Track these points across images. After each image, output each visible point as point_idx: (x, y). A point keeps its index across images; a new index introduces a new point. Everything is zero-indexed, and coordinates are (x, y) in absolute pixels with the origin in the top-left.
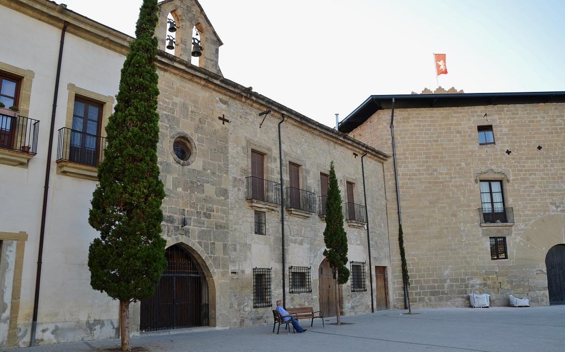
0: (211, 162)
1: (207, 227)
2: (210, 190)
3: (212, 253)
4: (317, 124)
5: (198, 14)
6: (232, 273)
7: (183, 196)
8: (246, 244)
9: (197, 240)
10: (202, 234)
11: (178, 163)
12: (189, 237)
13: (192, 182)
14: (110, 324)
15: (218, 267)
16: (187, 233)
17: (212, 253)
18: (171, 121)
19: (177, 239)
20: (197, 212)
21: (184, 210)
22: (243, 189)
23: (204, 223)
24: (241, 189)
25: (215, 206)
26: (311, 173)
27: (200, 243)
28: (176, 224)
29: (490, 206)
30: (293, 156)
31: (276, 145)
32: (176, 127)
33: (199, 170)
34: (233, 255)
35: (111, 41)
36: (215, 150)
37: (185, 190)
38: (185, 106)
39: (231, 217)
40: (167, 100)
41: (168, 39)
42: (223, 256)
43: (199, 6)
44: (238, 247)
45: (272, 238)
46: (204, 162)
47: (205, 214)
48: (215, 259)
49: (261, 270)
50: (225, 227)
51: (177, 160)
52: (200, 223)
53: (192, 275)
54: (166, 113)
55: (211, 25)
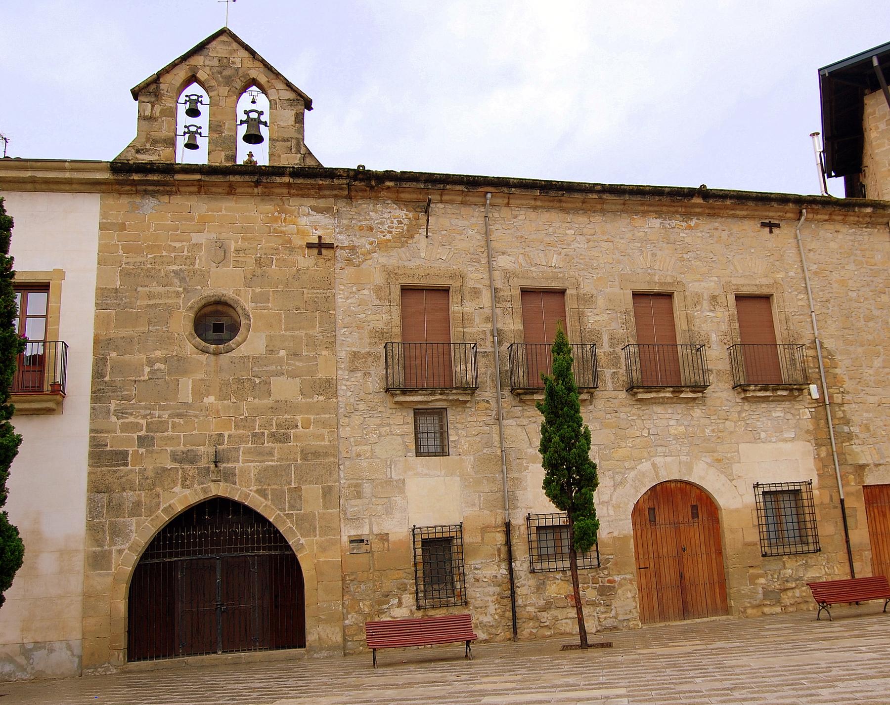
0: (288, 333)
1: (279, 460)
2: (285, 388)
3: (292, 507)
4: (599, 188)
5: (249, 63)
6: (351, 541)
7: (218, 411)
8: (389, 482)
9: (255, 488)
10: (265, 476)
11: (204, 351)
12: (235, 484)
13: (240, 381)
14: (65, 649)
15: (310, 531)
16: (229, 476)
17: (292, 507)
18: (188, 279)
19: (204, 490)
20: (254, 435)
22: (378, 371)
23: (271, 454)
24: (372, 372)
25: (298, 417)
26: (601, 302)
27: (262, 493)
28: (203, 464)
29: (423, 428)
30: (534, 275)
31: (479, 262)
32: (199, 287)
34: (353, 506)
35: (46, 181)
36: (298, 309)
37: (223, 397)
38: (222, 246)
39: (345, 432)
40: (178, 245)
41: (242, 122)
42: (321, 511)
43: (247, 48)
44: (367, 489)
45: (469, 460)
46: (270, 338)
47: (273, 435)
48: (301, 520)
50: (326, 454)
51: (200, 348)
52: (260, 454)
53: (261, 552)
54: (175, 267)
55: (278, 75)
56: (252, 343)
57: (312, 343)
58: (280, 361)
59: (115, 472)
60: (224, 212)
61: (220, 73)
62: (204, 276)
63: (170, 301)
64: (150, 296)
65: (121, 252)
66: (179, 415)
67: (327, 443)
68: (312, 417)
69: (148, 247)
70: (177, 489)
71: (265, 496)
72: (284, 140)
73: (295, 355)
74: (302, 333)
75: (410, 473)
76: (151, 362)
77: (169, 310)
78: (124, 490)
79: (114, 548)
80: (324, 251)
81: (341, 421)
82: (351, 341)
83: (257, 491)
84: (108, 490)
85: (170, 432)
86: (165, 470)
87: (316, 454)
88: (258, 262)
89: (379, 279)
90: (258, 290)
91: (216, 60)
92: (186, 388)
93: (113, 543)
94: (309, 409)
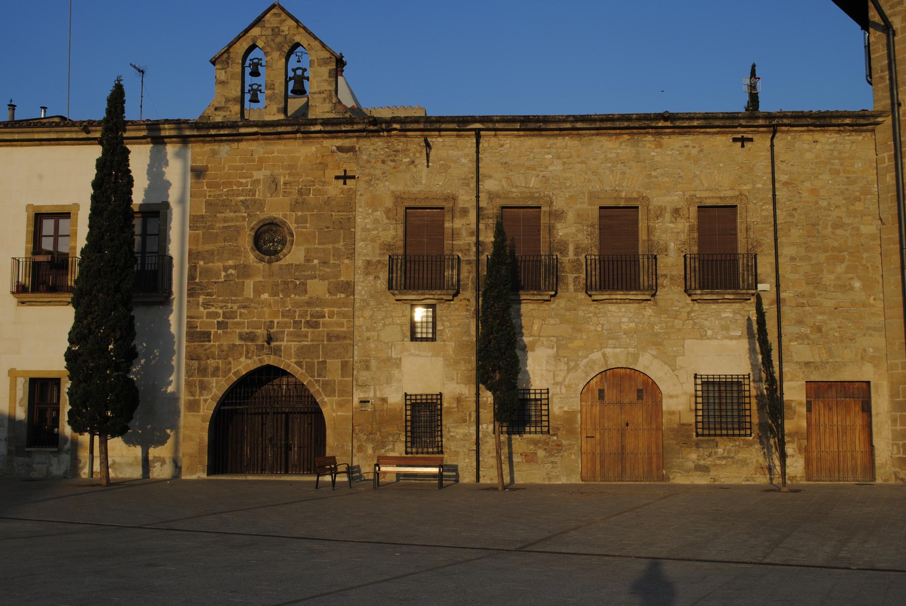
1: (312, 340)
2: (317, 288)
3: (319, 375)
4: (571, 119)
6: (361, 402)
8: (389, 359)
9: (293, 360)
10: (302, 352)
11: (262, 260)
13: (286, 283)
15: (332, 393)
16: (277, 351)
17: (319, 375)
20: (295, 322)
21: (272, 322)
22: (384, 275)
23: (306, 336)
25: (326, 310)
26: (571, 216)
27: (299, 364)
31: (468, 185)
33: (297, 263)
34: (363, 376)
36: (328, 228)
37: (274, 294)
38: (274, 181)
39: (359, 322)
40: (244, 181)
44: (373, 363)
46: (308, 251)
47: (307, 322)
48: (325, 384)
49: (419, 397)
50: (345, 338)
52: (298, 336)
54: (242, 198)
56: (295, 255)
57: (337, 254)
58: (314, 268)
59: (203, 346)
60: (276, 154)
61: (273, 40)
62: (261, 205)
63: (238, 224)
64: (225, 220)
65: (205, 188)
66: (245, 307)
67: (345, 329)
68: (336, 310)
69: (224, 183)
70: (243, 359)
71: (301, 367)
72: (320, 93)
73: (325, 263)
74: (330, 246)
75: (406, 353)
76: (226, 269)
77: (238, 230)
78: (208, 358)
79: (202, 398)
80: (348, 181)
81: (356, 314)
82: (366, 251)
83: (296, 363)
84: (198, 358)
85: (238, 319)
86: (234, 345)
87: (338, 337)
88: (300, 192)
89: (389, 203)
90: (299, 214)
91: (270, 30)
93: (201, 394)
94: (334, 303)
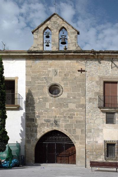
0: (73, 93)
1: (70, 122)
2: (72, 106)
3: (73, 133)
8: (98, 129)
10: (67, 126)
12: (59, 127)
13: (61, 104)
15: (78, 139)
17: (73, 133)
19: (52, 128)
21: (56, 116)
22: (97, 102)
23: (68, 121)
24: (95, 103)
25: (75, 113)
27: (66, 130)
28: (52, 122)
33: (65, 98)
37: (56, 107)
40: (45, 71)
44: (93, 130)
46: (68, 94)
47: (69, 117)
52: (65, 121)
54: (44, 76)
56: (64, 95)
57: (79, 95)
58: (71, 99)
59: (31, 123)
60: (56, 62)
61: (54, 26)
62: (51, 79)
63: (43, 84)
64: (38, 83)
65: (31, 73)
66: (46, 111)
67: (82, 119)
68: (79, 113)
69: (37, 71)
70: (46, 127)
71: (67, 131)
72: (72, 43)
73: (74, 98)
74: (77, 93)
75: (104, 128)
76: (39, 99)
77: (43, 87)
78: (33, 127)
79: (31, 139)
80: (82, 72)
81: (86, 114)
82: (89, 95)
83: (65, 129)
84: (30, 127)
85: (44, 115)
86: (43, 123)
87: (80, 122)
88: (65, 75)
89: (97, 79)
90: (65, 82)
91: (53, 22)
92: (48, 105)
93: (31, 138)
94: (78, 111)
